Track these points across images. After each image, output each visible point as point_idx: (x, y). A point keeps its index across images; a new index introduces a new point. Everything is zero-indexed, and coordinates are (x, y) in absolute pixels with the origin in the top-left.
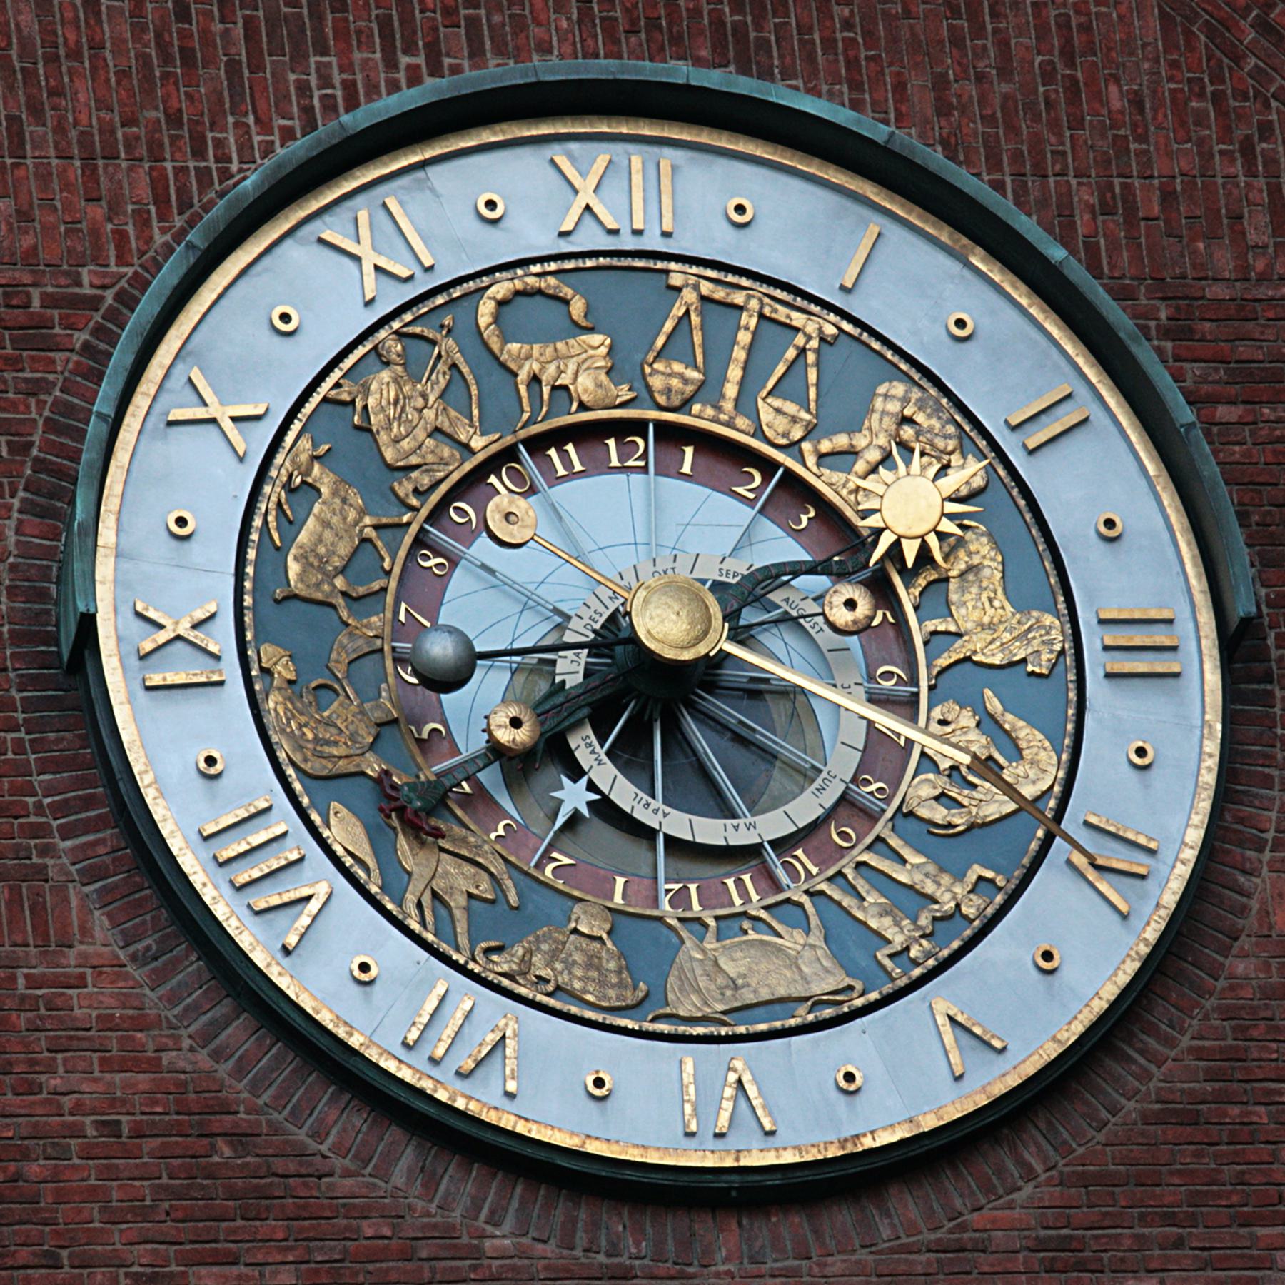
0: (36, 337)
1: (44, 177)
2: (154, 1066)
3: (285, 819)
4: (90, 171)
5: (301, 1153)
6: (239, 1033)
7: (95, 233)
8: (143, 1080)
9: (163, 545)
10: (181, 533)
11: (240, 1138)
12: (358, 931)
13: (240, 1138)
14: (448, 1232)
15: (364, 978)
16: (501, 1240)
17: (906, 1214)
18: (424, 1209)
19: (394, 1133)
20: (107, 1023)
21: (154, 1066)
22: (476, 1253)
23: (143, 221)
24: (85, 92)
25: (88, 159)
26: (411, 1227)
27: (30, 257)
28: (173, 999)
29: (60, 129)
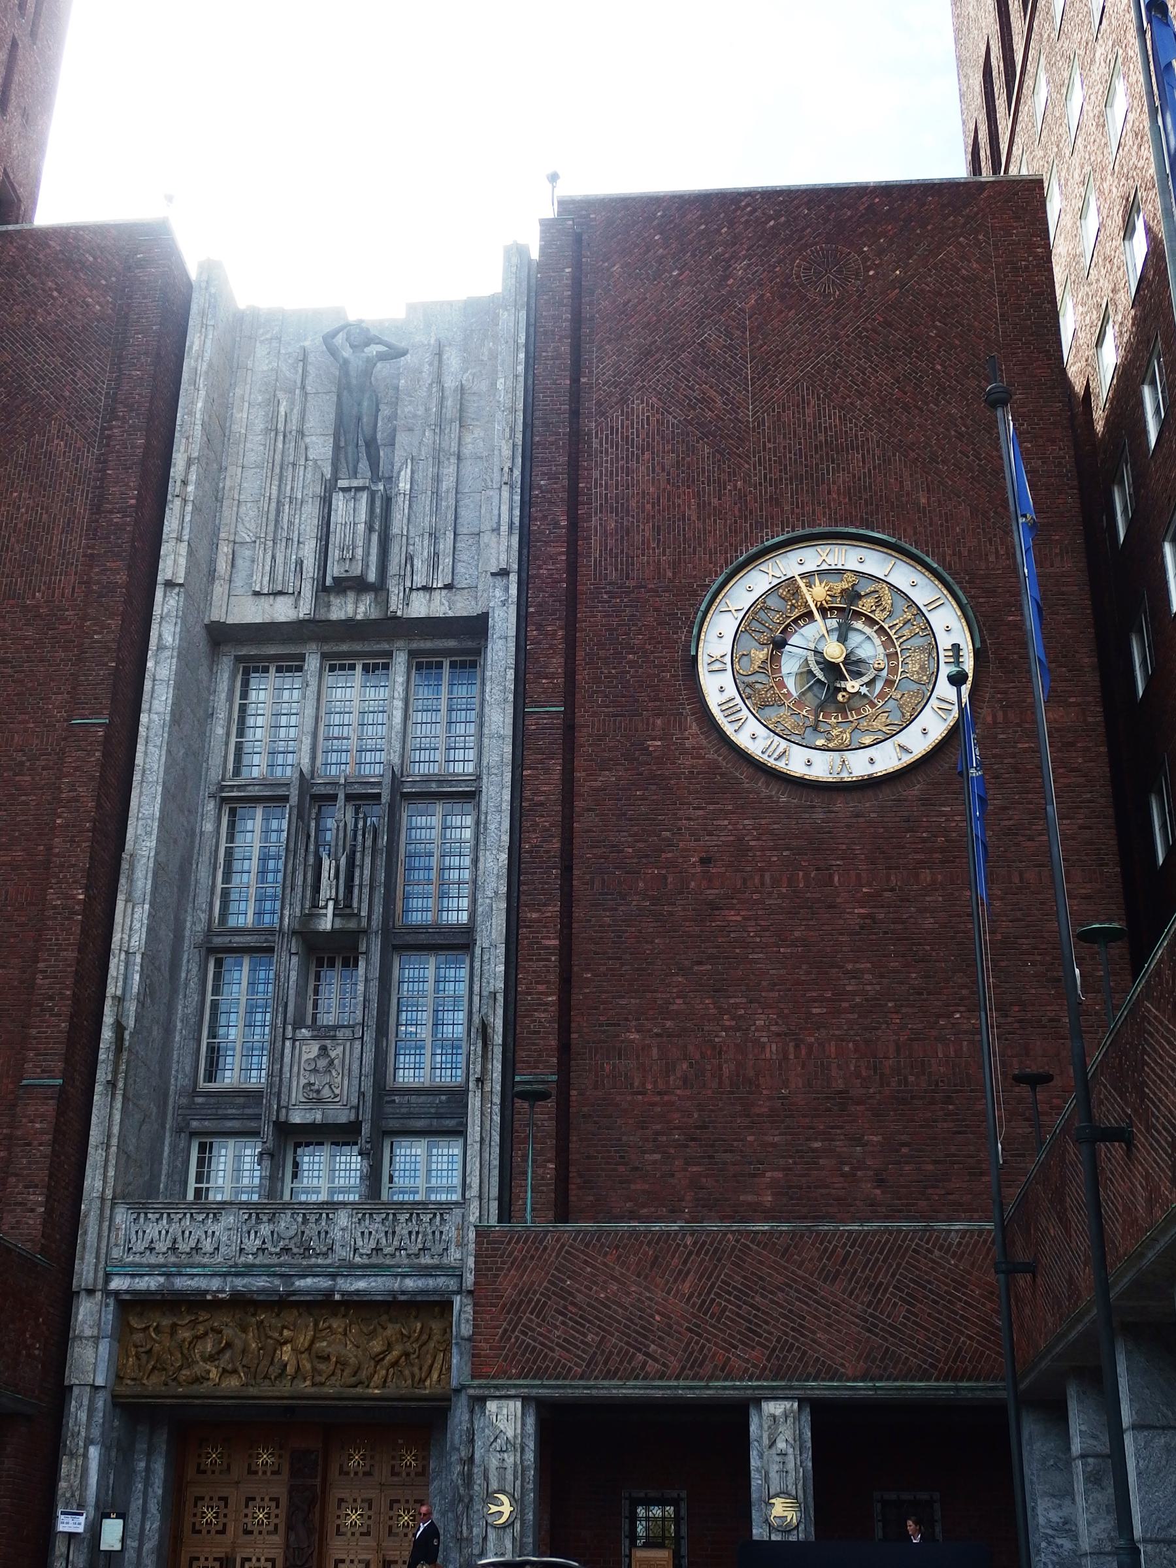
0: (694, 594)
1: (700, 559)
2: (703, 758)
3: (738, 700)
4: (710, 557)
5: (737, 778)
6: (724, 751)
7: (710, 570)
8: (701, 761)
9: (718, 636)
10: (720, 636)
11: (722, 775)
12: (753, 725)
13: (722, 775)
14: (771, 797)
15: (754, 737)
16: (784, 799)
17: (886, 794)
18: (765, 792)
19: (760, 773)
20: (694, 748)
21: (703, 758)
22: (778, 802)
23: (721, 567)
24: (711, 540)
25: (710, 554)
26: (763, 795)
27: (695, 577)
28: (709, 742)
29: (705, 549)
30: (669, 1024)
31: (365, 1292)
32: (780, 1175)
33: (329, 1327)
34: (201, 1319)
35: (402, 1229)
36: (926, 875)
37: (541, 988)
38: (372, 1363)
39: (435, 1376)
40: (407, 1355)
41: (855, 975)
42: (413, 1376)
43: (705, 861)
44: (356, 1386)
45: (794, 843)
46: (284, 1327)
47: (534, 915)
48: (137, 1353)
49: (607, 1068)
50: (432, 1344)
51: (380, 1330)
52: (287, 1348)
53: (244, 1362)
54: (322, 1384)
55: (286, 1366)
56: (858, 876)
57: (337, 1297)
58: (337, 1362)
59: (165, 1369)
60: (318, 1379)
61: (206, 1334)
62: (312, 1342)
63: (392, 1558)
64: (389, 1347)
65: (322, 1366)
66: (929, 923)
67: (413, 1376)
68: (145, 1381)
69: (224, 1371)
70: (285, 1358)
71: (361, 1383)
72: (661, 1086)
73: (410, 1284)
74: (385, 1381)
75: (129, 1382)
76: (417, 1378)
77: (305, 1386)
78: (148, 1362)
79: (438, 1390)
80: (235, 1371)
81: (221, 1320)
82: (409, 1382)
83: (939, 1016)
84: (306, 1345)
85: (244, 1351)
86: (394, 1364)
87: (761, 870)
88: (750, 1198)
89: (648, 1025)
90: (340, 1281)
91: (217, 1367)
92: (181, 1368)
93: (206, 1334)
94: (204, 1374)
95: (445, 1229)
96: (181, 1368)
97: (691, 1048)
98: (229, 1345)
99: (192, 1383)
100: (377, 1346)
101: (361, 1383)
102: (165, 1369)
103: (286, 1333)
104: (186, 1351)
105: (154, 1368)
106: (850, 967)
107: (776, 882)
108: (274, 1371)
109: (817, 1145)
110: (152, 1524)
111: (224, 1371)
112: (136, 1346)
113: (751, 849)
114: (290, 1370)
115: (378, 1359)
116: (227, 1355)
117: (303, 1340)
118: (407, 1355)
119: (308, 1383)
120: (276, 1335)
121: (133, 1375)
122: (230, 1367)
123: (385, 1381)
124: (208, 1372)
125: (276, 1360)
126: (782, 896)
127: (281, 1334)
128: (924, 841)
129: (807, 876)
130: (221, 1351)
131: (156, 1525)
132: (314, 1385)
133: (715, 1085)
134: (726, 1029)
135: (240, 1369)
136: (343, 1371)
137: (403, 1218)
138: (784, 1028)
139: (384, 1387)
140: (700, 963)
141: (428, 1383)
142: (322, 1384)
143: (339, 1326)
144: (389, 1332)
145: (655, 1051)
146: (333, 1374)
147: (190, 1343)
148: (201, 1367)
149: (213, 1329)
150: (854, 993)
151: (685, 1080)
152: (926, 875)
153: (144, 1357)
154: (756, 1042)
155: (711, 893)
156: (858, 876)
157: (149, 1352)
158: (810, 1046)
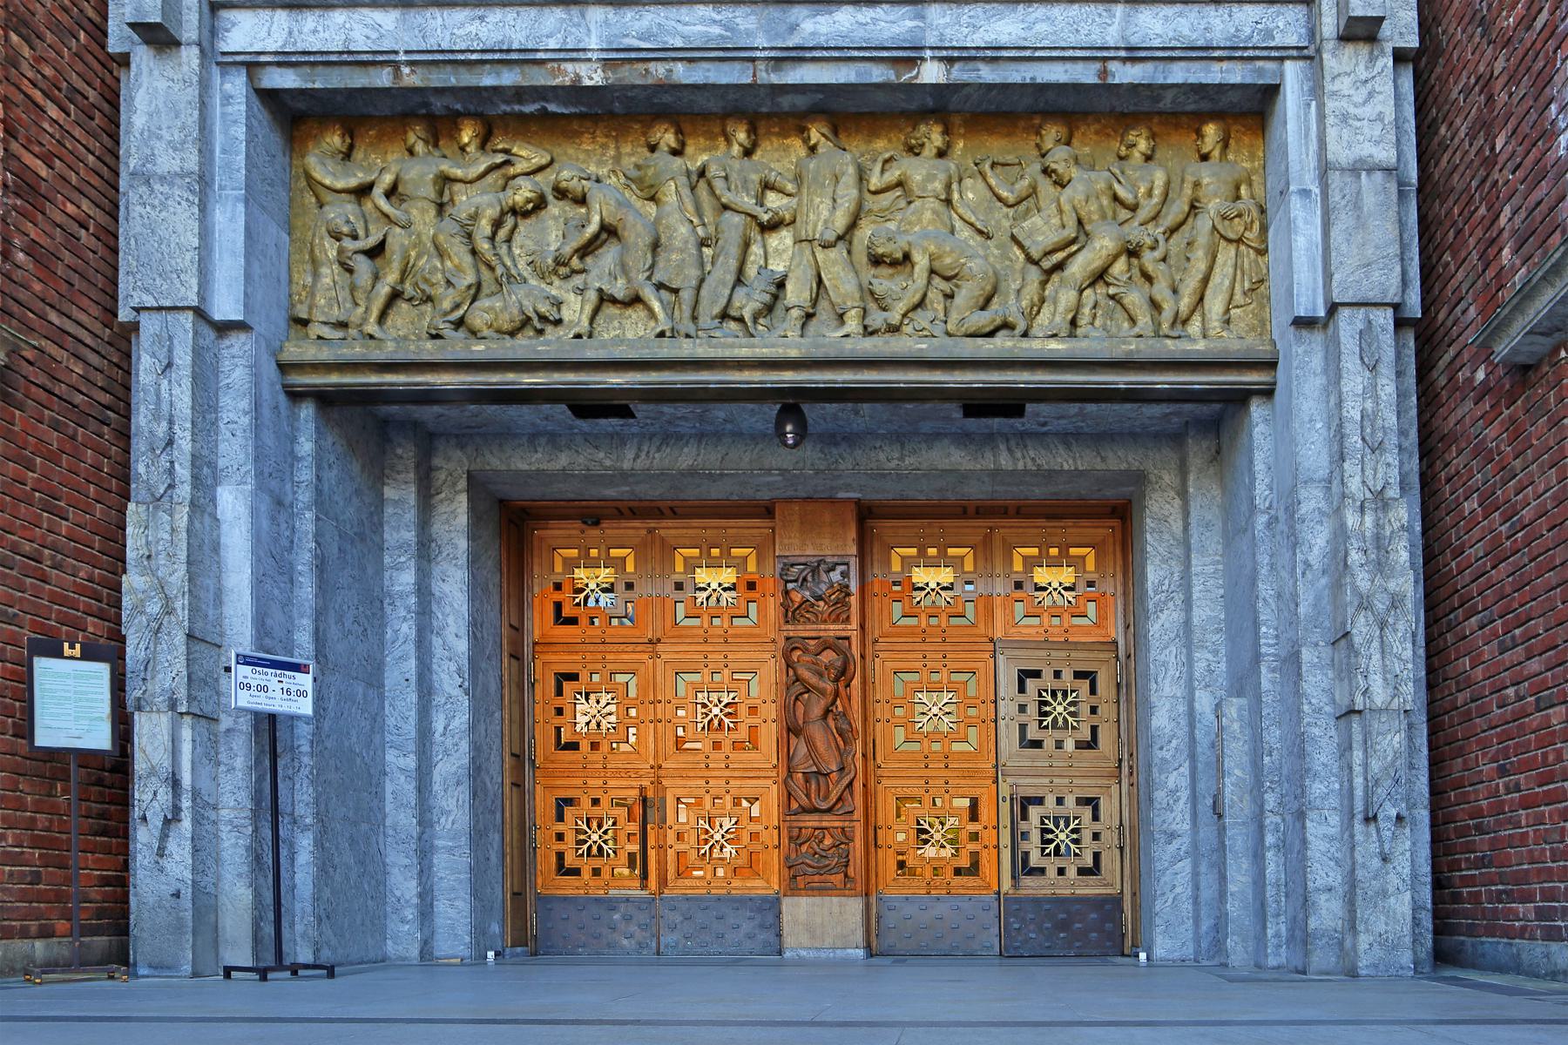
33: (900, 184)
34: (520, 167)
38: (1034, 275)
39: (1215, 306)
42: (1155, 305)
44: (991, 334)
46: (767, 186)
48: (341, 251)
50: (1203, 224)
51: (1046, 187)
52: (782, 240)
53: (657, 277)
54: (894, 329)
55: (781, 285)
58: (932, 272)
59: (429, 299)
60: (877, 319)
61: (540, 204)
62: (853, 226)
63: (1031, 793)
64: (1083, 232)
65: (884, 282)
67: (1155, 305)
68: (371, 328)
69: (604, 299)
70: (778, 266)
71: (1006, 326)
74: (1073, 323)
75: (326, 332)
76: (1167, 315)
77: (844, 338)
78: (376, 278)
79: (1233, 343)
80: (636, 300)
81: (589, 163)
82: (1144, 320)
84: (840, 222)
85: (655, 246)
86: (1100, 276)
91: (581, 291)
92: (476, 291)
93: (540, 204)
94: (544, 308)
96: (476, 291)
98: (609, 231)
99: (512, 334)
100: (1043, 230)
101: (1006, 326)
102: (429, 299)
103: (773, 200)
104: (484, 246)
105: (395, 296)
108: (746, 304)
110: (449, 719)
111: (604, 299)
112: (337, 236)
114: (797, 293)
116: (609, 256)
117: (825, 215)
118: (1133, 253)
119: (852, 325)
120: (747, 201)
121: (336, 314)
122: (619, 289)
123: (1073, 323)
124: (558, 304)
125: (751, 271)
127: (760, 202)
130: (585, 250)
131: (461, 720)
132: (868, 332)
135: (649, 294)
136: (949, 296)
139: (1072, 335)
141: (1194, 327)
142: (894, 329)
143: (930, 178)
144: (1074, 194)
146: (920, 304)
147: (497, 224)
148: (531, 295)
149: (561, 193)
153: (363, 265)
157: (376, 252)
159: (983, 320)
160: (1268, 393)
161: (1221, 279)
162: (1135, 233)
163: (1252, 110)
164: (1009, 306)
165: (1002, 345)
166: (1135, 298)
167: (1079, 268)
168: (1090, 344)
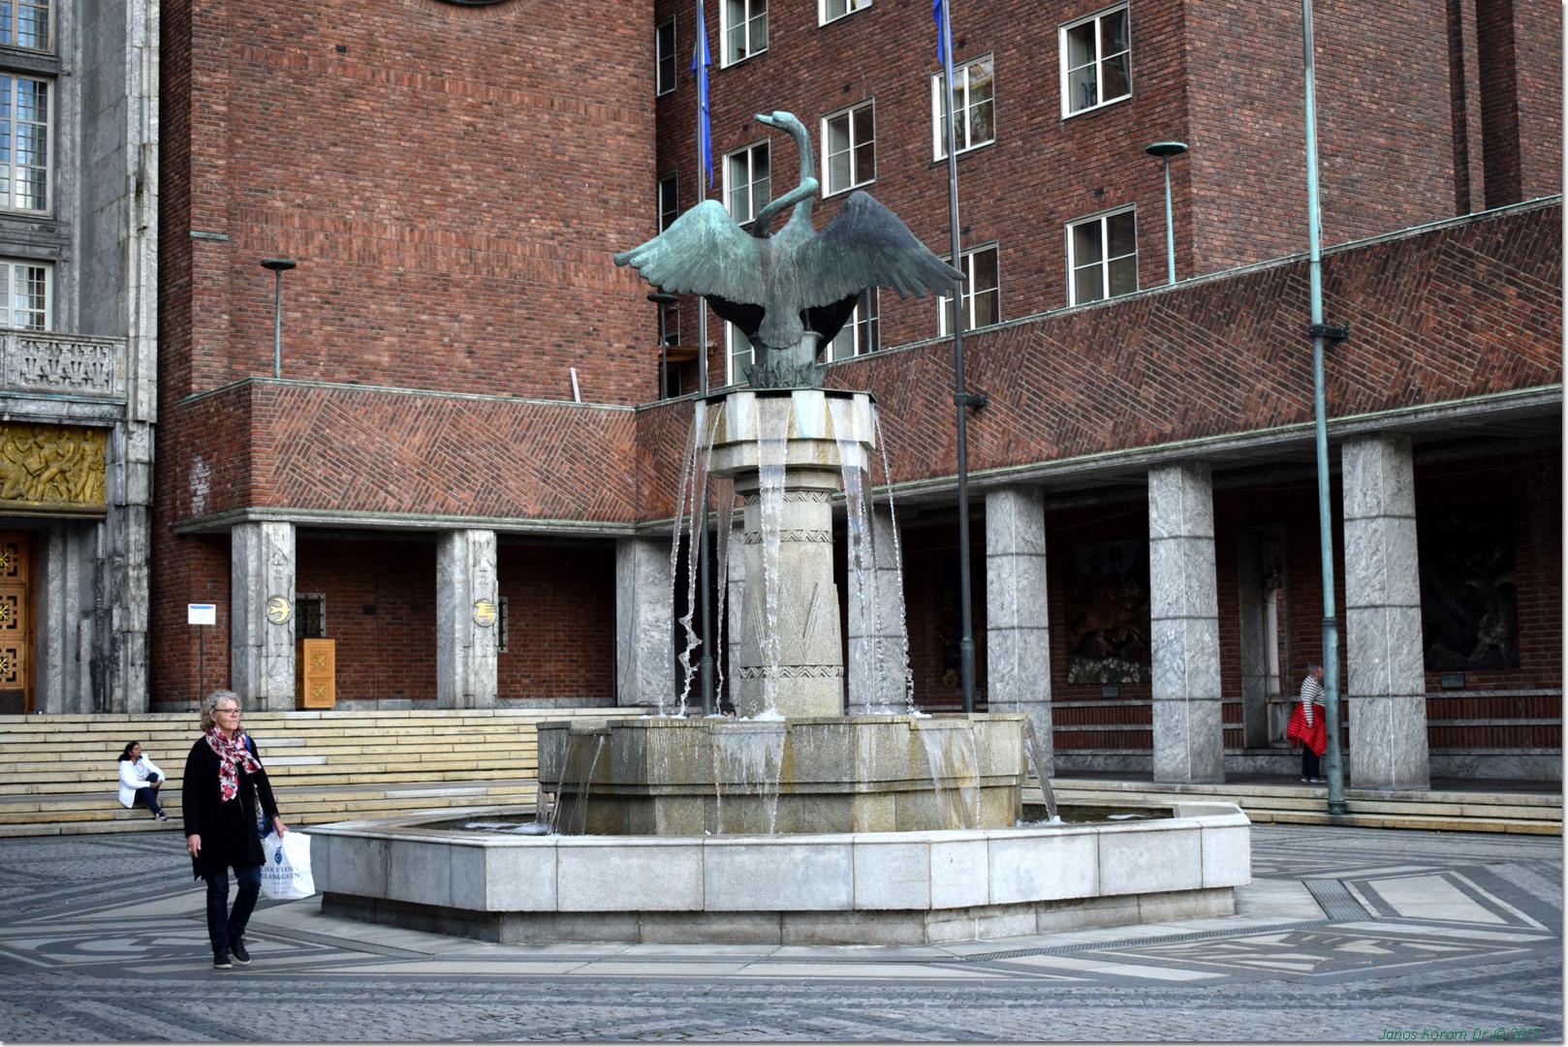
30: (309, 197)
31: (36, 415)
32: (395, 340)
35: (66, 358)
36: (516, 95)
37: (212, 151)
39: (88, 492)
40: (62, 472)
41: (459, 174)
43: (342, 49)
45: (415, 46)
47: (206, 79)
49: (257, 230)
50: (86, 464)
51: (35, 448)
56: (465, 87)
57: (6, 418)
64: (47, 467)
66: (516, 138)
72: (302, 253)
73: (77, 410)
83: (520, 220)
86: (52, 480)
87: (388, 67)
88: (372, 358)
89: (291, 195)
90: (10, 402)
95: (106, 362)
97: (327, 221)
100: (34, 463)
106: (455, 167)
107: (399, 80)
109: (425, 317)
113: (379, 45)
115: (36, 475)
118: (62, 472)
126: (403, 94)
128: (516, 64)
129: (424, 79)
133: (345, 256)
134: (356, 208)
137: (66, 348)
138: (401, 214)
140: (335, 145)
144: (45, 452)
145: (297, 221)
150: (457, 191)
151: (322, 249)
152: (516, 95)
154: (379, 222)
155: (346, 81)
156: (465, 87)
158: (422, 232)
159: (13, 493)
160: (104, 521)
161: (90, 483)
162: (65, 467)
163: (107, 431)
164: (22, 488)
165: (19, 502)
166: (63, 488)
167: (46, 475)
168: (48, 504)
